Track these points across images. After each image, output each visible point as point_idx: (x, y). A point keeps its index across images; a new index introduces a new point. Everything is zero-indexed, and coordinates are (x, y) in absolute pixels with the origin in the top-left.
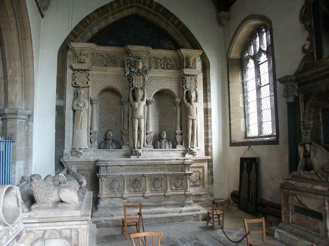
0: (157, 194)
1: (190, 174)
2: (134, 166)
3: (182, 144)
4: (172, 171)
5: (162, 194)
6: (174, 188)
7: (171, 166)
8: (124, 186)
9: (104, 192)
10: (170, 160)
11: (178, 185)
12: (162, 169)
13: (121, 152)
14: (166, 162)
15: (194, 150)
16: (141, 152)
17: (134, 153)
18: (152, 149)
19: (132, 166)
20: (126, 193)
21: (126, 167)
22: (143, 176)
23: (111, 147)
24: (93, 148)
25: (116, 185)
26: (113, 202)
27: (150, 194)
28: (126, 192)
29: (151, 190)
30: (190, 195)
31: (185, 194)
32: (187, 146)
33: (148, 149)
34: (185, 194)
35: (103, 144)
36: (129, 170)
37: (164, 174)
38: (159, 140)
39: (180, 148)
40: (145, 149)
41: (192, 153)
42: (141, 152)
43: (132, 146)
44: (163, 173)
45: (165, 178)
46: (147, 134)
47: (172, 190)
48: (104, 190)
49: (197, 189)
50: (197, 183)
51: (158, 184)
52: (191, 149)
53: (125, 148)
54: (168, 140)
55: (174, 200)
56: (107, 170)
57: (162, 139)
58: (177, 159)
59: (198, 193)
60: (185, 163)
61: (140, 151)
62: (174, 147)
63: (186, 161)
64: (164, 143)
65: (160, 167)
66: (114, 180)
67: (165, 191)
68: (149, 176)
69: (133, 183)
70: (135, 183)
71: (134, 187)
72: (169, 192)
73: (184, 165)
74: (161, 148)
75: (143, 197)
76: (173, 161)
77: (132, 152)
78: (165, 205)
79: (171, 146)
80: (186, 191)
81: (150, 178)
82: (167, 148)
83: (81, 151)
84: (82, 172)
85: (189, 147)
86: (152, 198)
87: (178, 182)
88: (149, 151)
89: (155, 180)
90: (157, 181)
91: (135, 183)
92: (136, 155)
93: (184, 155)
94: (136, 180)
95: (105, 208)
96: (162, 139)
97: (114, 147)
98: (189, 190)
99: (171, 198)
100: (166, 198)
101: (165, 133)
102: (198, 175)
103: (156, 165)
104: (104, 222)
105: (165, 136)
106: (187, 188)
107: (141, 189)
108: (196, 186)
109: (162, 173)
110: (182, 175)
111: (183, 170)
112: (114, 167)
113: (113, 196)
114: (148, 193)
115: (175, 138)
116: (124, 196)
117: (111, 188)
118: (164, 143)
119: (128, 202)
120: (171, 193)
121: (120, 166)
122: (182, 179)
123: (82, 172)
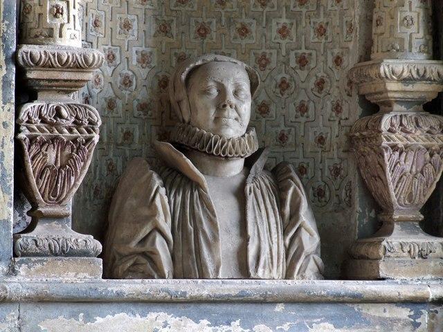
18: (83, 276)
38: (177, 179)
46: (25, 91)
54: (276, 166)
57: (209, 151)
62: (344, 259)
64: (225, 209)
74: (189, 264)
79: (310, 240)
88: (42, 300)
96: (209, 151)
101: (235, 75)
105: (236, 127)
115: (362, 143)
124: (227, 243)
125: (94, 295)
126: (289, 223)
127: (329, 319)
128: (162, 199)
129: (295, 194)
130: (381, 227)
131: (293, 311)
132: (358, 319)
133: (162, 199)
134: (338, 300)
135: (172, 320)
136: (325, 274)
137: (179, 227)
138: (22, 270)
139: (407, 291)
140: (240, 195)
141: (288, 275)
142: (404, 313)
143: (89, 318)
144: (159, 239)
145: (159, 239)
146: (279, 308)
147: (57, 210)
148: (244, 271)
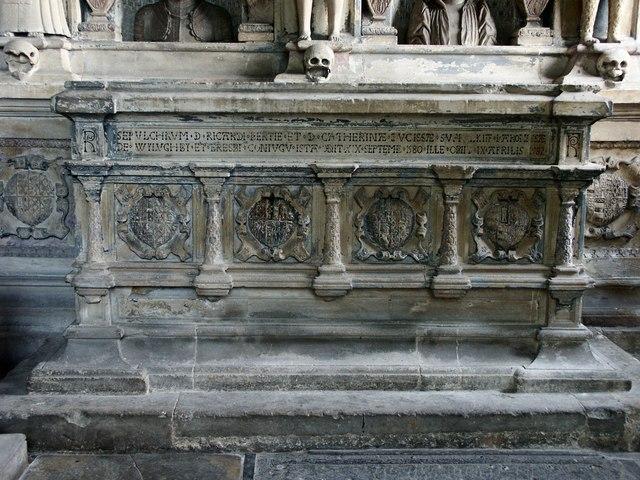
0: (385, 280)
1: (586, 178)
2: (260, 116)
3: (546, 20)
4: (481, 153)
5: (419, 279)
6: (484, 250)
7: (477, 126)
8: (207, 231)
9: (99, 259)
10: (469, 89)
11: (506, 234)
12: (421, 141)
13: (231, 56)
14: (447, 103)
15: (616, 52)
16: (331, 56)
17: (294, 60)
18: (391, 42)
19: (250, 116)
20: (218, 267)
21: (220, 122)
22: (314, 175)
23: (183, 31)
24: (94, 36)
25: (165, 221)
26: (146, 311)
27: (349, 279)
28: (218, 260)
29: (356, 258)
30: (574, 294)
31: (545, 289)
32: (573, 32)
33: (367, 44)
34: (545, 289)
35: (147, 20)
36: (236, 141)
37: (433, 170)
39: (538, 41)
40: (353, 43)
41: (604, 69)
42: (331, 56)
43: (291, 28)
44: (425, 164)
45: (434, 192)
47: (473, 259)
48: (97, 244)
49: (614, 255)
50: (615, 229)
51: (395, 225)
52: (599, 46)
53: (252, 37)
55: (480, 313)
56: (115, 138)
58: (511, 89)
59: (616, 277)
60: (559, 111)
61: (324, 51)
62: (506, 37)
63: (565, 97)
64: (452, 17)
65: (409, 129)
66: (153, 193)
67: (435, 263)
68: (348, 176)
69: (258, 213)
70: (271, 212)
71: (261, 236)
72: (458, 275)
73: (555, 126)
74: (436, 39)
75: (312, 290)
76: (487, 97)
77: (288, 55)
78: (431, 343)
79: (491, 30)
80: (554, 273)
81: (351, 190)
82: (470, 44)
83: (25, 46)
84: (36, 151)
85: (589, 36)
86: (363, 299)
87: (509, 220)
89: (380, 202)
90: (391, 208)
91: (271, 212)
92: (303, 70)
93: (555, 73)
94: (272, 199)
95: (102, 341)
97: (201, 30)
98: (570, 264)
99: (470, 303)
100: (438, 304)
102: (624, 184)
103: (385, 118)
104: (76, 420)
106: (560, 254)
107: (303, 249)
108: (607, 240)
109: (423, 163)
110: (536, 180)
111: (545, 151)
112: (150, 121)
113: (146, 278)
114: (339, 272)
116: (204, 281)
117: (137, 236)
118: (452, 17)
119: (232, 314)
120: (468, 280)
121: (187, 116)
122: (536, 202)
123: (36, 151)
124: (453, 31)
125: (393, 51)
126: (481, 22)
127: (494, 61)
128: (426, 12)
129: (484, 11)
130: (523, 24)
131: (478, 58)
132: (505, 62)
133: (426, 12)
134: (498, 54)
135: (426, 62)
136: (495, 44)
137: (433, 25)
138: (364, 41)
139: (529, 51)
140: (460, 12)
141: (480, 44)
142: (528, 59)
143: (391, 60)
144: (424, 29)
145: (424, 29)
146: (473, 57)
147: (381, 17)
148: (459, 43)
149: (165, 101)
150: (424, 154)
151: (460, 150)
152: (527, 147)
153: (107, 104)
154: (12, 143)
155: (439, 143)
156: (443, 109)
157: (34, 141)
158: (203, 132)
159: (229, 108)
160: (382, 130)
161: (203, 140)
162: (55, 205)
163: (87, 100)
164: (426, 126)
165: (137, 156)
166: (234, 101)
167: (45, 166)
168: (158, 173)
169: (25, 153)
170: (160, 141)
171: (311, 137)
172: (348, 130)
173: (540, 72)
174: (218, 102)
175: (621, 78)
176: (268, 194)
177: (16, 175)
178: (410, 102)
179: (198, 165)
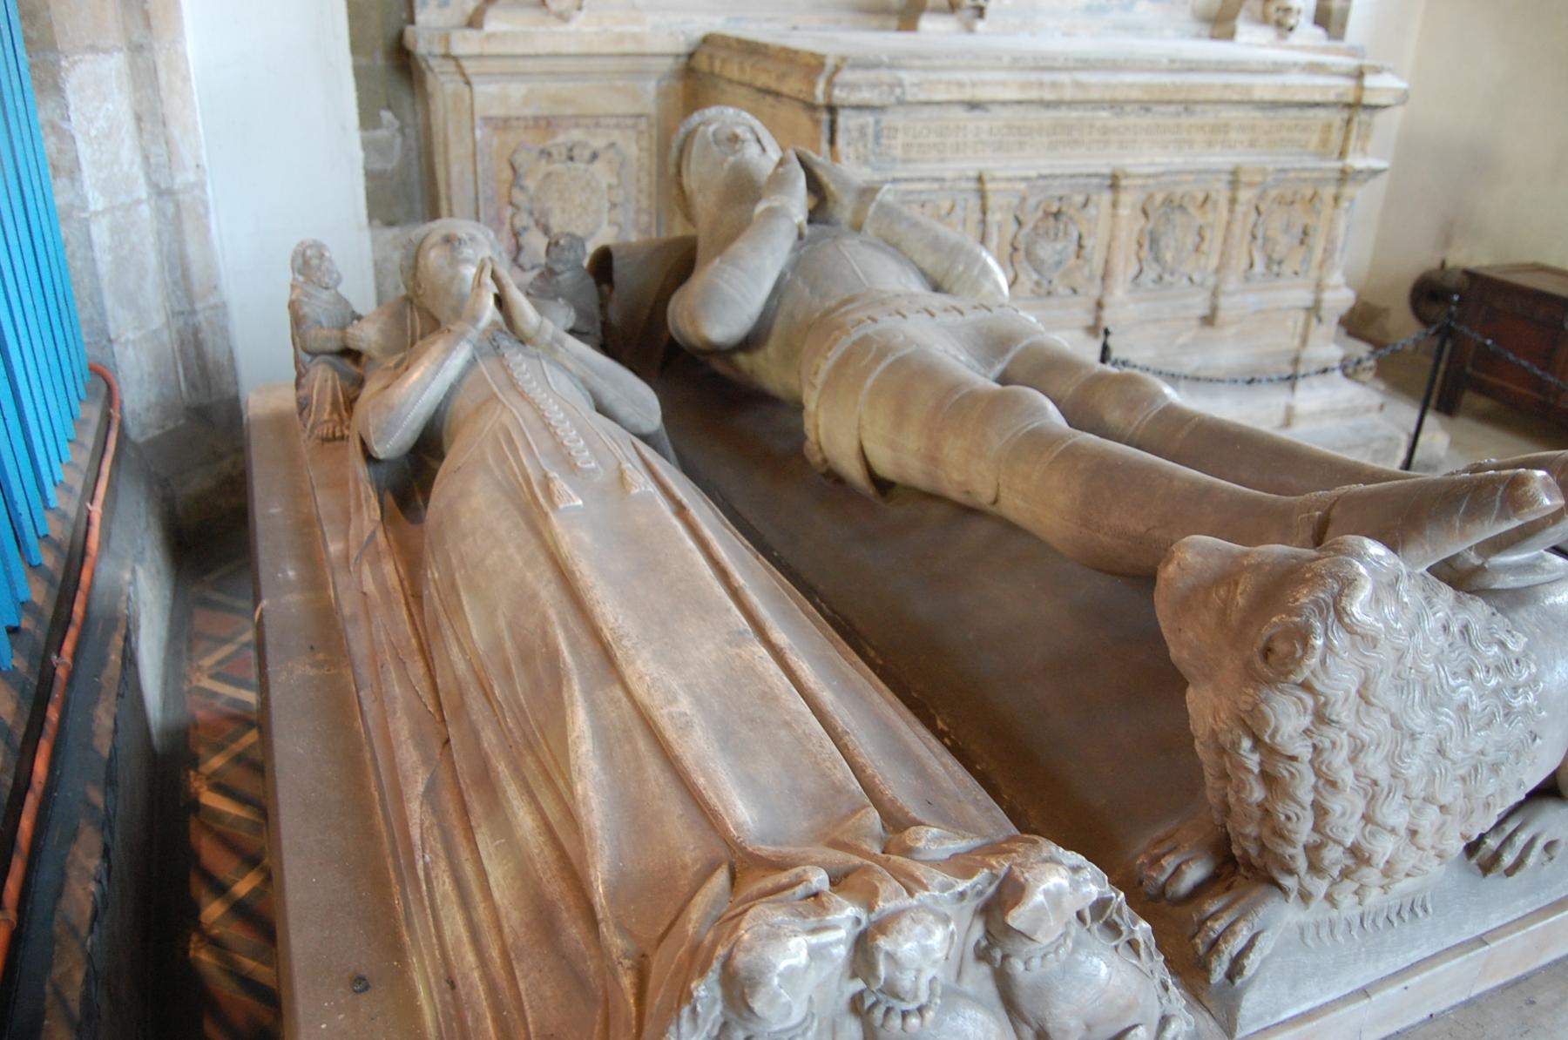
84: (576, 135)
123: (576, 135)
149: (961, 85)
150: (1217, 149)
151: (1252, 144)
152: (1315, 139)
153: (898, 91)
154: (543, 123)
155: (1233, 135)
156: (1258, 95)
157: (577, 120)
158: (984, 125)
159: (1034, 94)
160: (1186, 121)
161: (984, 137)
162: (605, 217)
163: (874, 85)
164: (1227, 114)
165: (906, 161)
166: (1041, 84)
167: (594, 156)
168: (936, 186)
169: (561, 138)
170: (933, 139)
171: (1105, 131)
172: (1147, 120)
173: (1194, 12)
174: (1025, 86)
175: (1291, 29)
176: (1054, 209)
177: (548, 175)
178: (1226, 86)
179: (998, 174)
